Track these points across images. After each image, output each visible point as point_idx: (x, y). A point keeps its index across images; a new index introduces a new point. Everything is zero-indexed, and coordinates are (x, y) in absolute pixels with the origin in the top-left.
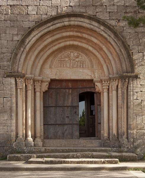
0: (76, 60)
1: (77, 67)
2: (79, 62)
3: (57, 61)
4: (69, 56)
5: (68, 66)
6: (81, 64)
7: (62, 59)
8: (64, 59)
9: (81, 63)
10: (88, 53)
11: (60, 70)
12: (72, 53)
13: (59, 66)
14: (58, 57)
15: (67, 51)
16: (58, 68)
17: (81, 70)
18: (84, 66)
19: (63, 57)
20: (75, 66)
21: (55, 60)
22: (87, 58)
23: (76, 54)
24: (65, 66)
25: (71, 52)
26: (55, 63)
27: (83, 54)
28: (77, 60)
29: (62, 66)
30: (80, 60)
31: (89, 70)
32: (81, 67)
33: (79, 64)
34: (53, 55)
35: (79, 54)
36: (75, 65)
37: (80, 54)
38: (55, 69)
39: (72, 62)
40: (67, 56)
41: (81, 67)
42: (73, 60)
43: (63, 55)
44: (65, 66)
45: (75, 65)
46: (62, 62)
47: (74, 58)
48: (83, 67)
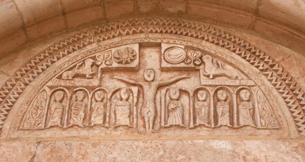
0: (183, 84)
1: (192, 123)
2: (202, 96)
3: (40, 90)
4: (135, 64)
5: (123, 120)
6: (222, 109)
7: (79, 82)
8: (95, 82)
9: (217, 100)
10: (262, 47)
11: (60, 144)
12: (151, 58)
13: (56, 120)
14: (50, 71)
15: (116, 40)
16: (48, 134)
17: (223, 145)
18: (244, 118)
19: (87, 69)
20: (175, 119)
21: (29, 89)
22: (258, 71)
23: (177, 54)
24: (97, 119)
25: (142, 46)
26: (29, 103)
27: (220, 49)
28: (190, 84)
29: (78, 120)
30: (205, 81)
31: (283, 139)
32: (224, 120)
33: (204, 108)
34: (20, 61)
35: (200, 53)
36: (178, 112)
37: (204, 52)
38: (14, 140)
39: (149, 92)
40: (115, 65)
41: (224, 120)
42: (160, 87)
43: (89, 62)
44: (97, 119)
45: (178, 112)
46: (80, 95)
47: (166, 77)
48: (234, 125)
